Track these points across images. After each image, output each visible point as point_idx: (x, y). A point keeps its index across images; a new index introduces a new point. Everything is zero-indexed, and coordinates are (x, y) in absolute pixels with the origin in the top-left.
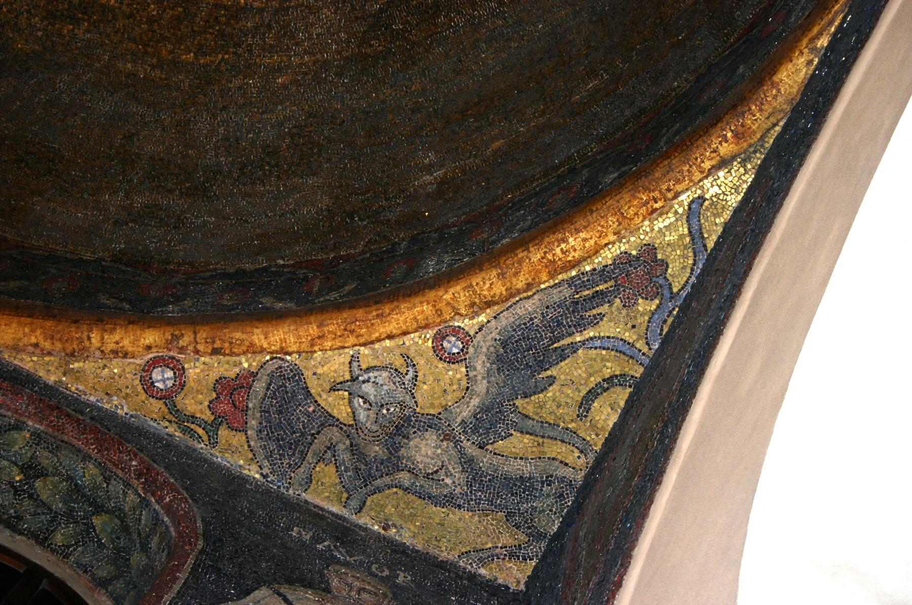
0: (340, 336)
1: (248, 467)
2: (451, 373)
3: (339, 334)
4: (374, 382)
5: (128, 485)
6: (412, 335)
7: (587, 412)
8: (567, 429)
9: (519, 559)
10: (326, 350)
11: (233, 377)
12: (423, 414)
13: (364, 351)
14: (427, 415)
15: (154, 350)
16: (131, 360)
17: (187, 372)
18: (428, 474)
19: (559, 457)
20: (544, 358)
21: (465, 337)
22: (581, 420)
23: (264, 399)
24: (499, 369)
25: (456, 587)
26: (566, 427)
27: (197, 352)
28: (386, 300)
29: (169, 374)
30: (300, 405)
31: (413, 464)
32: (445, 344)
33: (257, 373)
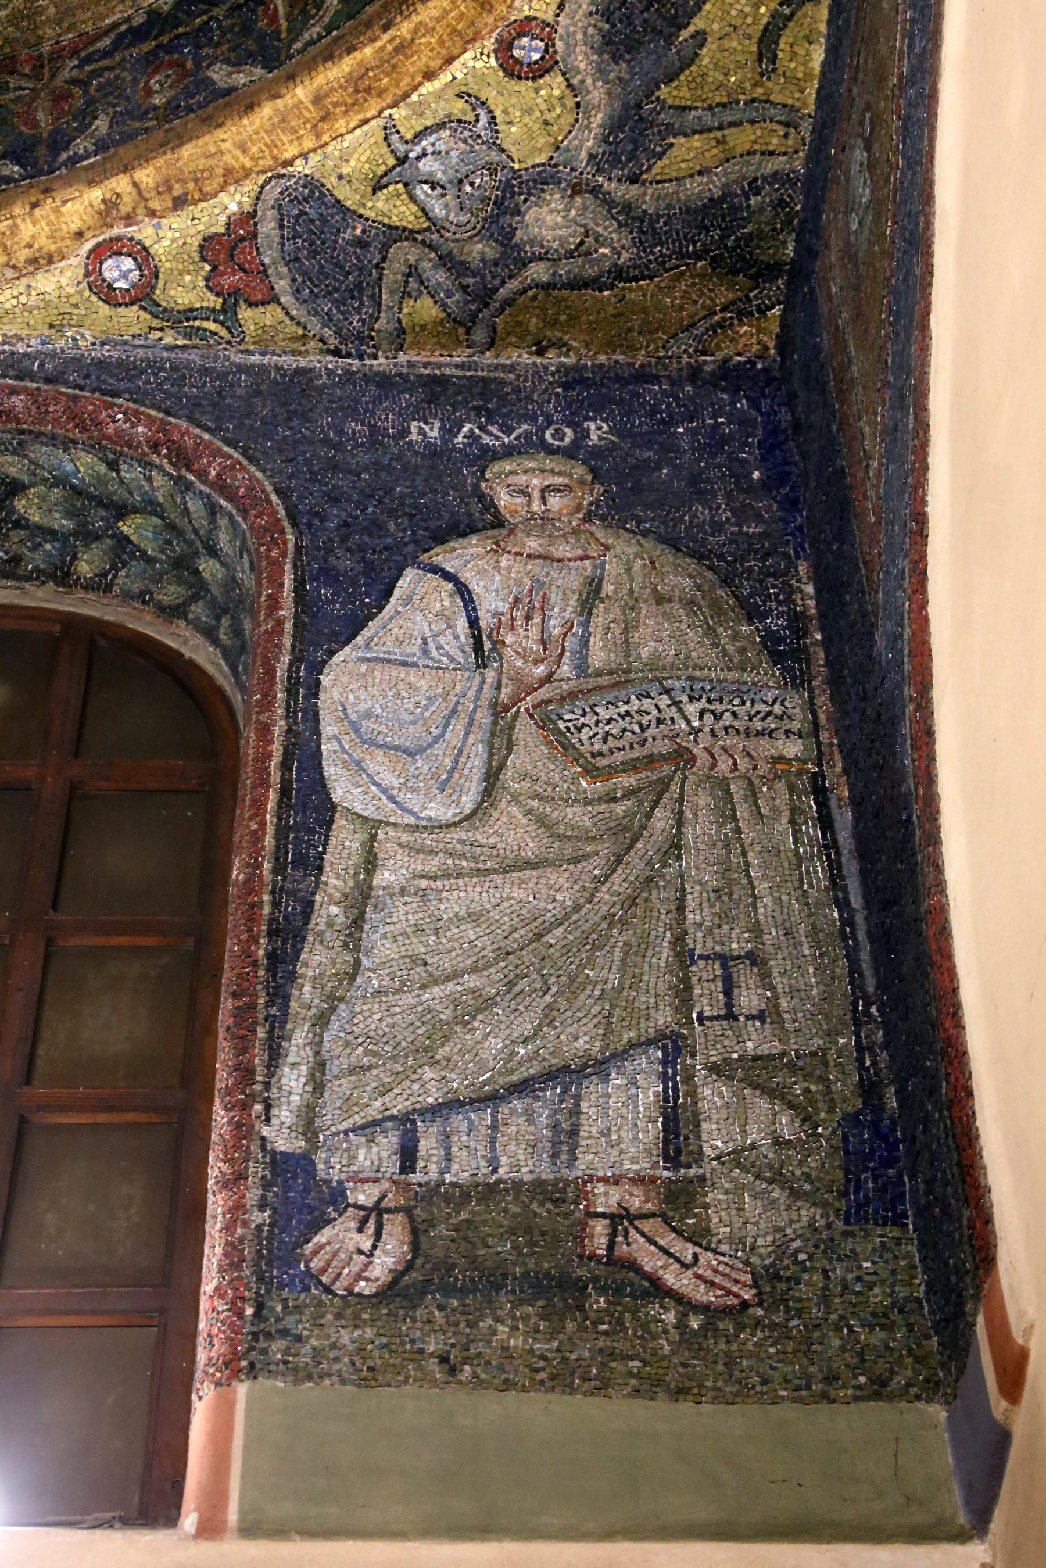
0: (354, 105)
1: (303, 349)
2: (543, 92)
3: (350, 101)
4: (433, 153)
5: (148, 465)
6: (462, 59)
7: (774, 63)
8: (753, 100)
9: (753, 315)
10: (342, 135)
11: (222, 230)
12: (526, 169)
13: (398, 113)
14: (533, 167)
15: (88, 234)
16: (63, 264)
17: (152, 251)
18: (571, 252)
19: (756, 147)
20: (676, 10)
21: (543, 29)
22: (769, 79)
23: (283, 245)
24: (613, 57)
25: (678, 406)
26: (749, 98)
27: (152, 214)
28: (399, 19)
29: (128, 263)
30: (339, 231)
31: (542, 246)
32: (516, 53)
33: (255, 211)
